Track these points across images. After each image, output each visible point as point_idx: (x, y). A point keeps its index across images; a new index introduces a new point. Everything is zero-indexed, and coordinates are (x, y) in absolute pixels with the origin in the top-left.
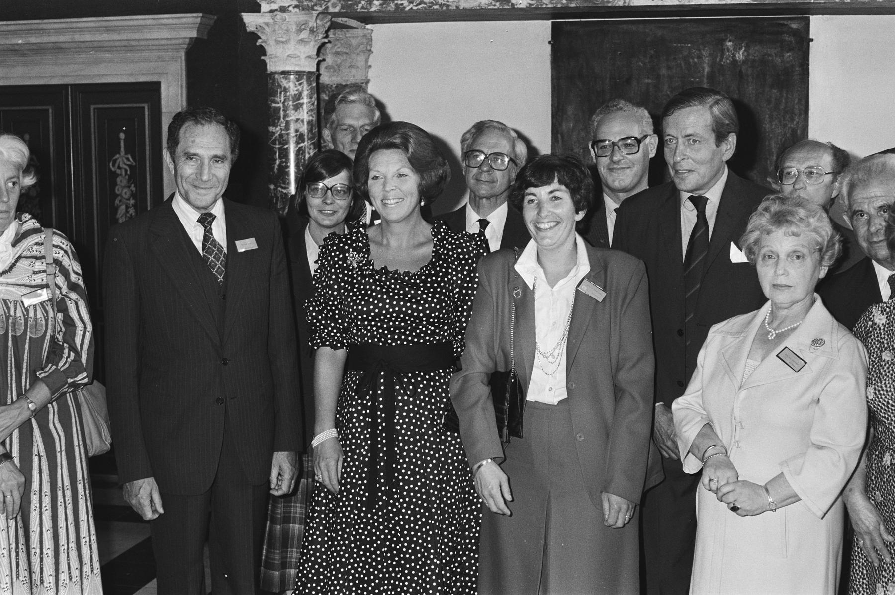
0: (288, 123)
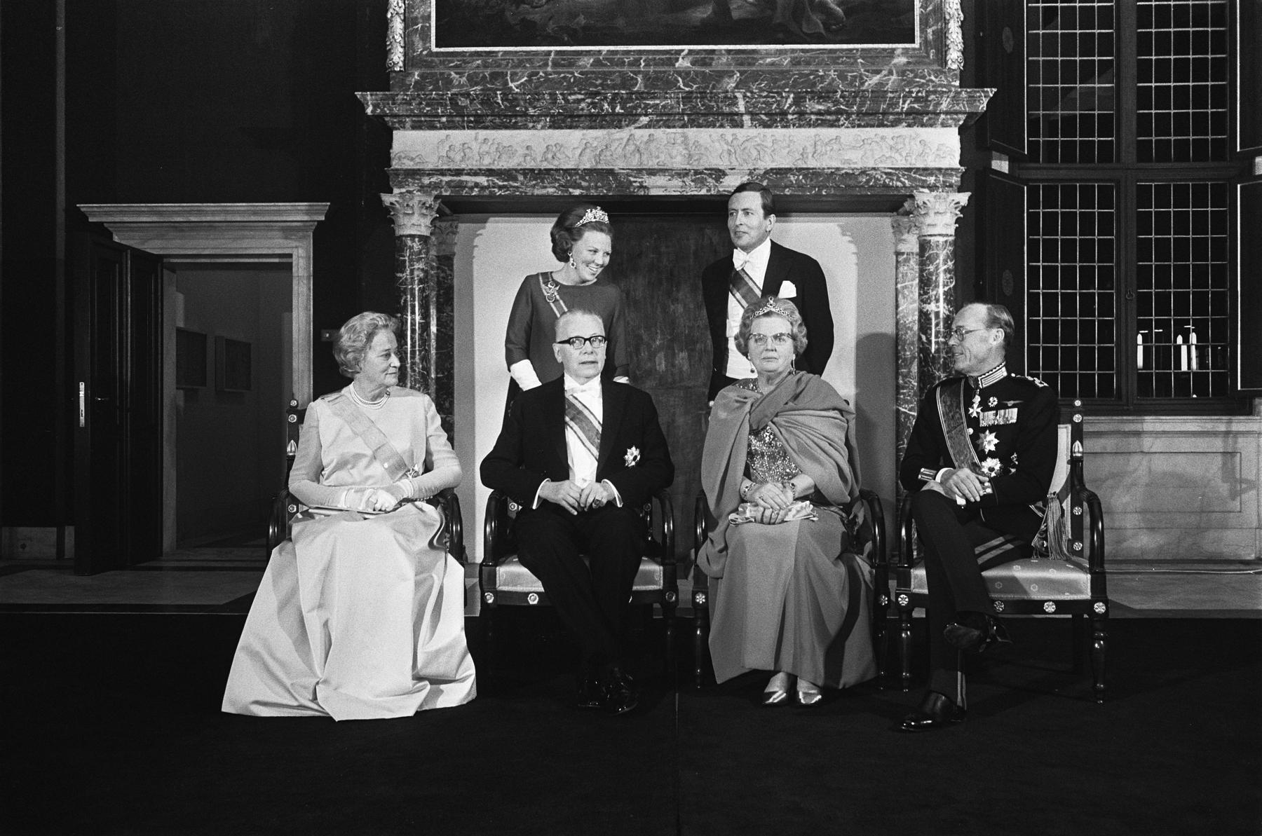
0: (412, 272)
